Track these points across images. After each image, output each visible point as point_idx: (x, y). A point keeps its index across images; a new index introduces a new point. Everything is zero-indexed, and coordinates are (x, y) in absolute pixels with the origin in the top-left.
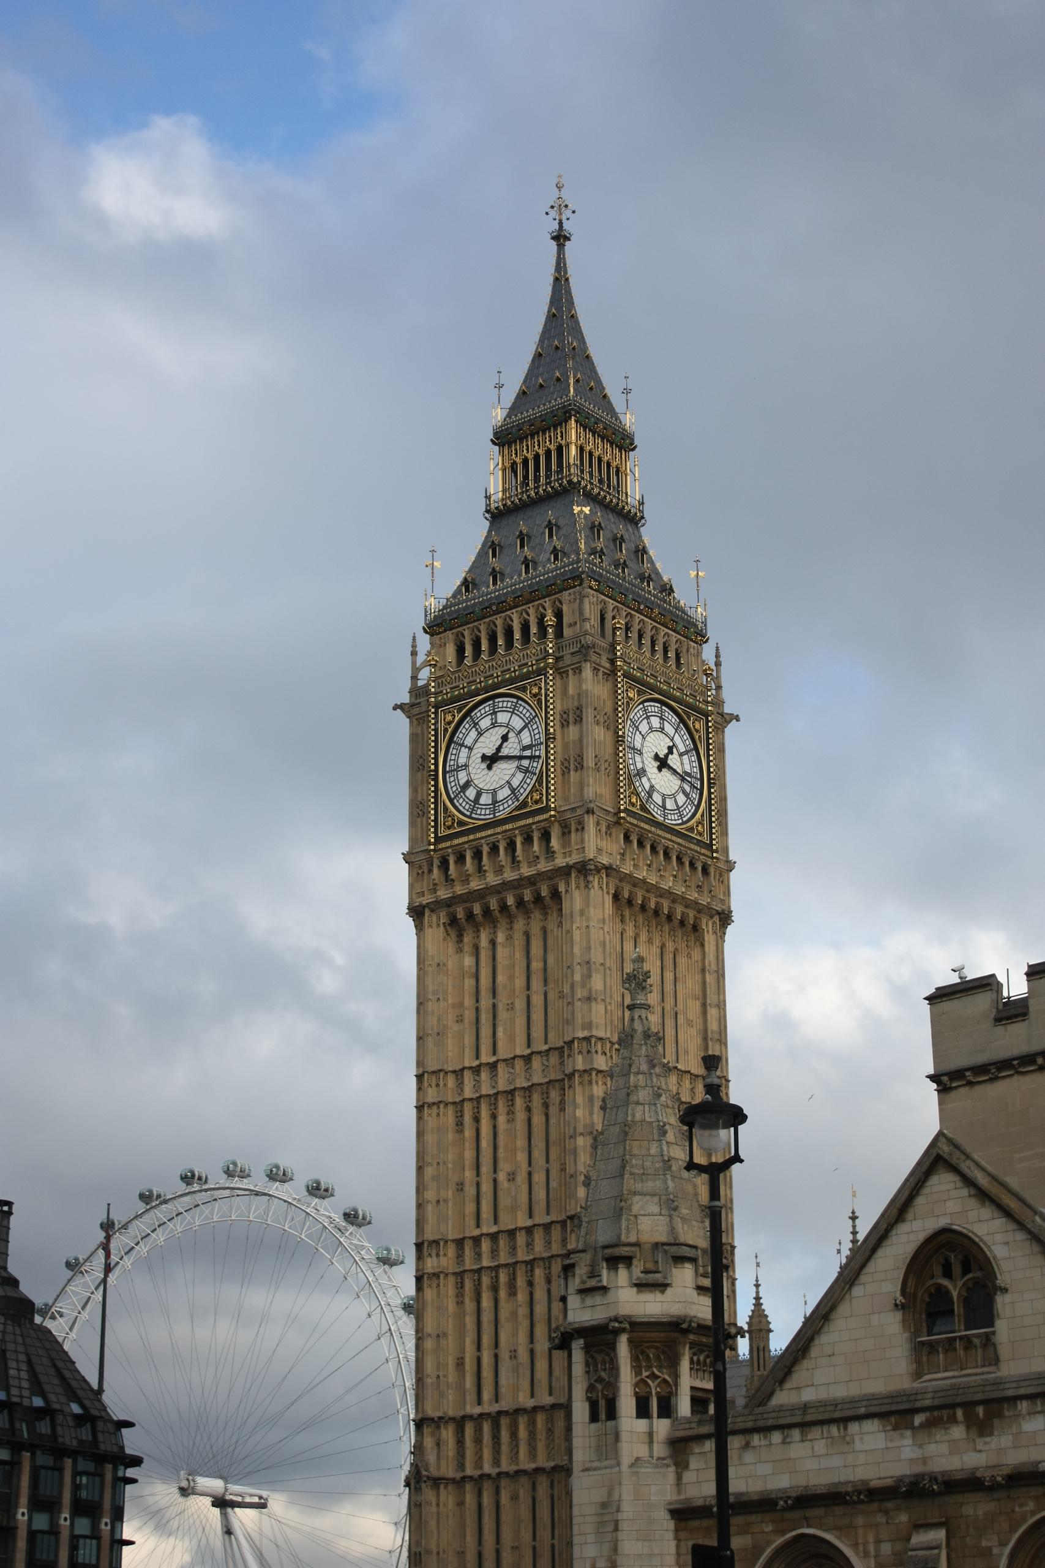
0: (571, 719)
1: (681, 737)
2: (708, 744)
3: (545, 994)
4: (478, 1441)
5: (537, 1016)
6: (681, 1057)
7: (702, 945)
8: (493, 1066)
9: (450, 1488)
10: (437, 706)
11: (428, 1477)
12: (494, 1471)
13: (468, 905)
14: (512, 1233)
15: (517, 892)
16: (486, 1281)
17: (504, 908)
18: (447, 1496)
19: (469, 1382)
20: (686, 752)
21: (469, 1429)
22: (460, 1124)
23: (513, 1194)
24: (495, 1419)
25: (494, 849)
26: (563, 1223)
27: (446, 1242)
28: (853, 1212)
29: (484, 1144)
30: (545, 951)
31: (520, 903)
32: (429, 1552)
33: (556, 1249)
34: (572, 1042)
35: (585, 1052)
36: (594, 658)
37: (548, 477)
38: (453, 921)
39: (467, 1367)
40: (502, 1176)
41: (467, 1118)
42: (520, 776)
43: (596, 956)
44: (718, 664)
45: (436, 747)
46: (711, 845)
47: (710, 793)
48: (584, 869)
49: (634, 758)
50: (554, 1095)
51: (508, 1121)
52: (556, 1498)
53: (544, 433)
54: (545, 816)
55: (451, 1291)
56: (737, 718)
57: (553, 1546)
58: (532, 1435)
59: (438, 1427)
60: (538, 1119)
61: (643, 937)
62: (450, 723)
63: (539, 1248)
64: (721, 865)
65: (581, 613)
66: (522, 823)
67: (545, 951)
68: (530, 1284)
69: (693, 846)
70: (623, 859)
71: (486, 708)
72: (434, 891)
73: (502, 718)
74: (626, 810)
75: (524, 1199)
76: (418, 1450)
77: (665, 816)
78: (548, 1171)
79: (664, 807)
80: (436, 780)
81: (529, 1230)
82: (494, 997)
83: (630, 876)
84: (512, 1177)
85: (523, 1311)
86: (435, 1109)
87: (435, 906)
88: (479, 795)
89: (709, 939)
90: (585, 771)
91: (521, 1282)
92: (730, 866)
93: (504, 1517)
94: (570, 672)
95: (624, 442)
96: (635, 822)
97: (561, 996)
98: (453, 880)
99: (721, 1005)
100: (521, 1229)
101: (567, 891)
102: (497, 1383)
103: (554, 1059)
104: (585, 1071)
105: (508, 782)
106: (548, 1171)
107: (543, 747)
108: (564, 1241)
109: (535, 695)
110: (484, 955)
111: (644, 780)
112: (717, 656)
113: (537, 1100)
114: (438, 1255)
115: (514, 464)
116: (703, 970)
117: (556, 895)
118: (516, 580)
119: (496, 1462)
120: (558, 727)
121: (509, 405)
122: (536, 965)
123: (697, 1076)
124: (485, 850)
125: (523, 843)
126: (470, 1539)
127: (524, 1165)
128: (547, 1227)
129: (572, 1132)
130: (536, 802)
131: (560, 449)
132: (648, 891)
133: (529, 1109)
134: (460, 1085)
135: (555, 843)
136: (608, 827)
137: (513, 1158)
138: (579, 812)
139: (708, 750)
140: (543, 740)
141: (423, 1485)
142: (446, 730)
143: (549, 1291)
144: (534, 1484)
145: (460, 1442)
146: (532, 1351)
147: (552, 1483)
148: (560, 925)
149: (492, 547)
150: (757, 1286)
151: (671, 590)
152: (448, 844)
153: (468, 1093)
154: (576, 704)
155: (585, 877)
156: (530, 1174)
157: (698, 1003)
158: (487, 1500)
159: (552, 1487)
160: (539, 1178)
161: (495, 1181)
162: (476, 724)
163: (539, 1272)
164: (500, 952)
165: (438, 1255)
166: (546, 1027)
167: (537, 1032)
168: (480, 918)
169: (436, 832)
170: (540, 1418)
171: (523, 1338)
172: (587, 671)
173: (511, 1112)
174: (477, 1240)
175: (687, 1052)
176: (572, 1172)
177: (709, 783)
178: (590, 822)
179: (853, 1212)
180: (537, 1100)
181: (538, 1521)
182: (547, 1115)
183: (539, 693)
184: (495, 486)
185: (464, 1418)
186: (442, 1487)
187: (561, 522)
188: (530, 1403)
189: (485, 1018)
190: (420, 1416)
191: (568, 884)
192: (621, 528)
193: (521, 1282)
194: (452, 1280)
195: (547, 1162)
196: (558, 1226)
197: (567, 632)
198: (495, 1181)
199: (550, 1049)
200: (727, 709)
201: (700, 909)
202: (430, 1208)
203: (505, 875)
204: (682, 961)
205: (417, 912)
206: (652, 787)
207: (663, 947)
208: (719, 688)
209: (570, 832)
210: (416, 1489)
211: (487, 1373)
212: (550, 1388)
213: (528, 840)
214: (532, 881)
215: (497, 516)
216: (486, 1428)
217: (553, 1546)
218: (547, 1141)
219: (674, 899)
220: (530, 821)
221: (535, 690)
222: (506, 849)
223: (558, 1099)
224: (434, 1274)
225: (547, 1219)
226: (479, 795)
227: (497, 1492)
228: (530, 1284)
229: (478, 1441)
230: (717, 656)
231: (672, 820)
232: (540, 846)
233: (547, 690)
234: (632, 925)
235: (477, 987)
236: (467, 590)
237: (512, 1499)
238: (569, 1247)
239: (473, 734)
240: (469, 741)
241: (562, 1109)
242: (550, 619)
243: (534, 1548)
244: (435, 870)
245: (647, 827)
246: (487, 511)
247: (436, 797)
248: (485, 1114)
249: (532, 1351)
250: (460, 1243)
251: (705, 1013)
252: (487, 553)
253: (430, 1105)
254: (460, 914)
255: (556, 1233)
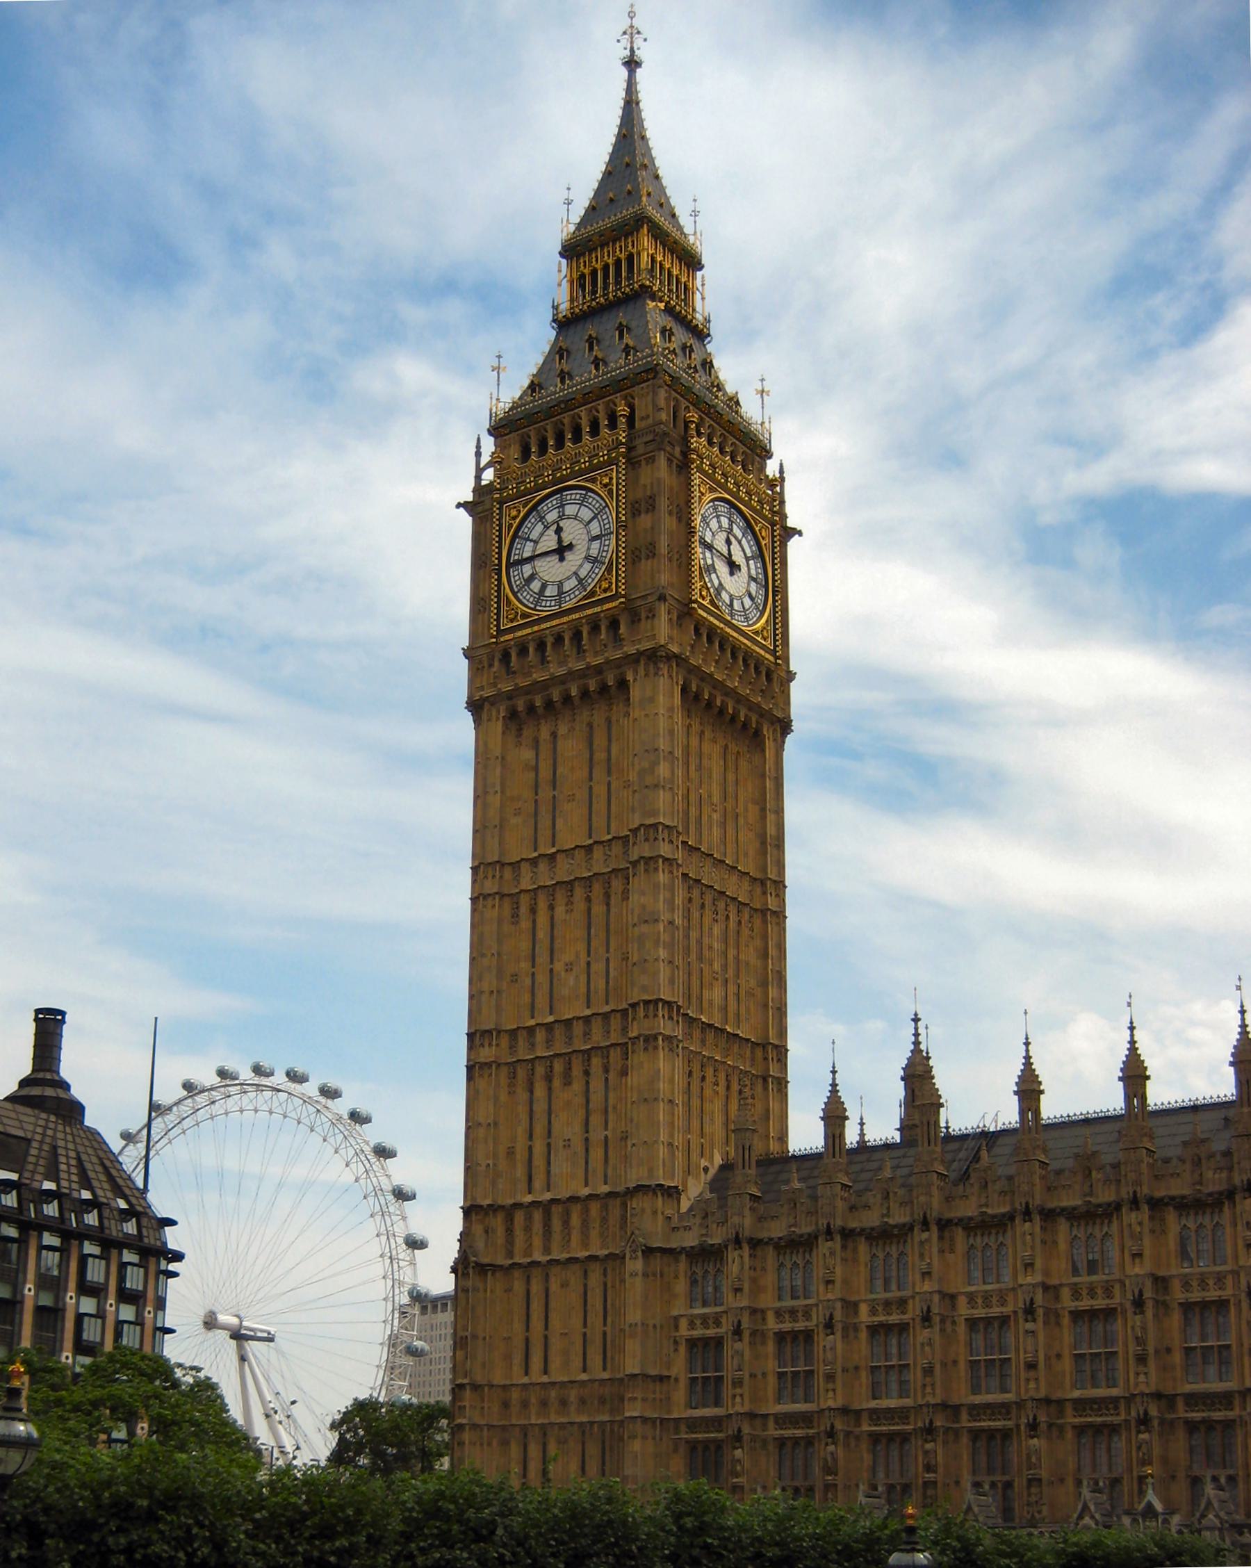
0: (643, 508)
1: (748, 542)
2: (774, 553)
3: (609, 784)
4: (528, 1229)
5: (600, 806)
6: (741, 858)
7: (763, 751)
8: (552, 857)
9: (498, 1274)
10: (501, 503)
11: (476, 1263)
12: (544, 1259)
13: (529, 697)
14: (568, 1023)
15: (582, 682)
16: (540, 1070)
17: (567, 699)
18: (495, 1284)
19: (520, 1172)
20: (753, 558)
21: (519, 1217)
22: (515, 916)
23: (571, 983)
24: (547, 1207)
25: (559, 639)
26: (624, 1012)
27: (499, 1032)
28: (916, 1014)
29: (541, 934)
30: (610, 741)
31: (585, 694)
32: (475, 1337)
33: (615, 1037)
34: (637, 829)
35: (652, 837)
36: (668, 449)
37: (618, 282)
38: (513, 715)
39: (518, 1157)
40: (559, 966)
41: (524, 909)
42: (588, 566)
43: (662, 744)
44: (782, 479)
45: (500, 542)
46: (775, 651)
47: (774, 601)
48: (654, 657)
49: (703, 553)
50: (617, 885)
51: (567, 911)
52: (609, 1285)
53: (614, 243)
54: (614, 604)
55: (504, 1081)
56: (800, 533)
57: (605, 1334)
58: (585, 1224)
59: (486, 1214)
60: (598, 909)
61: (708, 734)
62: (514, 518)
63: (598, 1037)
64: (783, 674)
65: (655, 405)
66: (589, 612)
67: (610, 741)
68: (587, 1073)
69: (758, 650)
70: (692, 652)
71: (553, 501)
72: (495, 685)
73: (570, 510)
74: (696, 601)
75: (583, 990)
76: (465, 1238)
77: (732, 615)
78: (608, 959)
79: (731, 605)
80: (499, 574)
81: (587, 1020)
82: (554, 789)
83: (698, 668)
84: (569, 968)
85: (580, 1100)
86: (490, 902)
87: (492, 701)
88: (544, 586)
89: (769, 745)
90: (655, 561)
91: (577, 1071)
92: (791, 676)
93: (552, 1305)
94: (643, 463)
95: (692, 262)
96: (705, 615)
97: (627, 785)
98: (514, 673)
99: (779, 811)
100: (579, 1018)
101: (635, 680)
102: (549, 1172)
103: (617, 848)
104: (651, 858)
105: (575, 573)
106: (608, 959)
107: (613, 537)
108: (625, 1030)
109: (606, 485)
110: (545, 749)
111: (713, 576)
112: (781, 471)
113: (597, 888)
114: (490, 1045)
115: (582, 276)
116: (763, 776)
117: (623, 684)
118: (586, 376)
119: (547, 1250)
120: (629, 515)
121: (578, 220)
122: (600, 756)
123: (755, 879)
124: (550, 641)
125: (589, 633)
126: (518, 1326)
127: (583, 955)
128: (606, 1016)
129: (636, 920)
130: (605, 591)
131: (630, 258)
132: (714, 688)
133: (588, 900)
134: (517, 878)
135: (622, 630)
136: (679, 618)
137: (572, 949)
138: (650, 599)
139: (774, 559)
140: (613, 528)
141: (471, 1271)
142: (511, 526)
143: (607, 1079)
144: (586, 1272)
145: (509, 1231)
146: (587, 1139)
147: (605, 1270)
148: (627, 714)
149: (559, 352)
150: (834, 1072)
151: (738, 403)
152: (511, 636)
153: (526, 884)
154: (649, 493)
155: (655, 664)
156: (588, 964)
157: (757, 807)
158: (536, 1287)
159: (605, 1275)
160: (598, 967)
161: (551, 970)
162: (542, 518)
163: (596, 1062)
164: (560, 744)
165: (490, 1045)
166: (609, 817)
167: (599, 821)
168: (540, 711)
169: (498, 626)
170: (595, 1208)
171: (578, 1127)
172: (662, 461)
173: (569, 903)
174: (531, 1030)
175: (746, 854)
176: (635, 960)
177: (774, 591)
178: (662, 609)
179: (916, 1014)
180: (597, 888)
181: (589, 1307)
182: (608, 905)
183: (610, 483)
184: (563, 296)
185: (517, 1206)
186: (489, 1273)
187: (633, 324)
188: (586, 1191)
189: (544, 812)
190: (468, 1204)
191: (636, 672)
192: (692, 341)
193: (577, 1071)
194: (504, 1070)
195: (608, 951)
196: (618, 1015)
197: (638, 424)
198: (551, 970)
199: (614, 838)
200: (790, 523)
201: (763, 714)
202: (485, 998)
203: (570, 665)
204: (743, 764)
205: (476, 706)
206: (720, 584)
207: (726, 747)
208: (782, 503)
209: (640, 620)
210: (463, 1274)
211: (539, 1161)
212: (606, 1176)
213: (595, 628)
214: (599, 670)
215: (564, 324)
216: (537, 1216)
217: (605, 1334)
218: (608, 931)
219: (739, 699)
220: (597, 609)
221: (606, 480)
222: (571, 639)
223: (621, 888)
224: (486, 1064)
225: (607, 1009)
226: (544, 586)
227: (547, 1278)
228: (587, 1073)
229: (528, 1229)
230: (781, 471)
231: (739, 622)
232: (607, 632)
233: (618, 478)
234: (698, 720)
235: (536, 781)
236: (533, 391)
237: (562, 1286)
238: (631, 1035)
239: (539, 527)
240: (534, 536)
241: (626, 898)
242: (622, 409)
243: (585, 1334)
244: (496, 663)
245: (716, 622)
246: (554, 321)
247: (499, 591)
248: (542, 905)
249: (587, 1139)
250: (513, 1033)
251: (763, 818)
252: (554, 360)
253: (486, 896)
254: (520, 705)
255: (616, 1022)
